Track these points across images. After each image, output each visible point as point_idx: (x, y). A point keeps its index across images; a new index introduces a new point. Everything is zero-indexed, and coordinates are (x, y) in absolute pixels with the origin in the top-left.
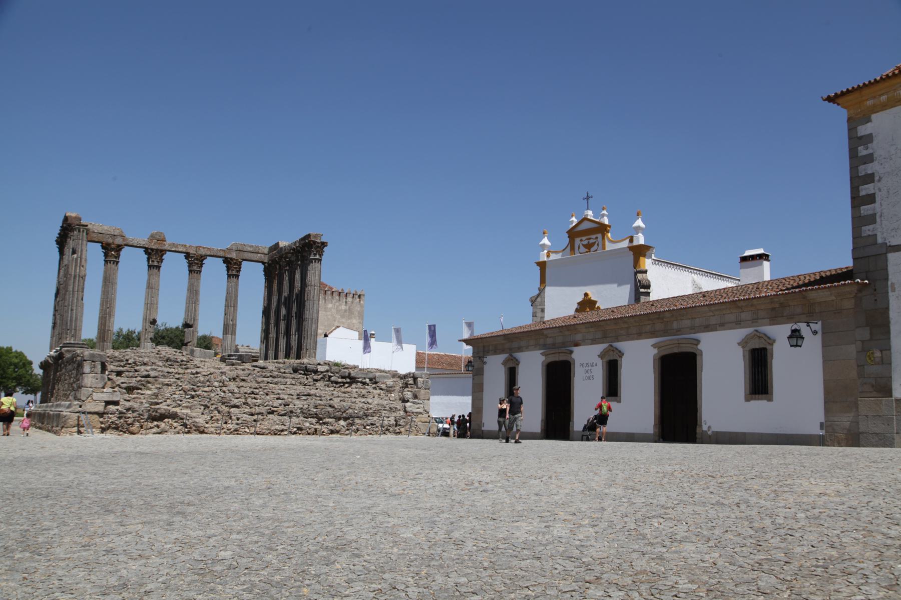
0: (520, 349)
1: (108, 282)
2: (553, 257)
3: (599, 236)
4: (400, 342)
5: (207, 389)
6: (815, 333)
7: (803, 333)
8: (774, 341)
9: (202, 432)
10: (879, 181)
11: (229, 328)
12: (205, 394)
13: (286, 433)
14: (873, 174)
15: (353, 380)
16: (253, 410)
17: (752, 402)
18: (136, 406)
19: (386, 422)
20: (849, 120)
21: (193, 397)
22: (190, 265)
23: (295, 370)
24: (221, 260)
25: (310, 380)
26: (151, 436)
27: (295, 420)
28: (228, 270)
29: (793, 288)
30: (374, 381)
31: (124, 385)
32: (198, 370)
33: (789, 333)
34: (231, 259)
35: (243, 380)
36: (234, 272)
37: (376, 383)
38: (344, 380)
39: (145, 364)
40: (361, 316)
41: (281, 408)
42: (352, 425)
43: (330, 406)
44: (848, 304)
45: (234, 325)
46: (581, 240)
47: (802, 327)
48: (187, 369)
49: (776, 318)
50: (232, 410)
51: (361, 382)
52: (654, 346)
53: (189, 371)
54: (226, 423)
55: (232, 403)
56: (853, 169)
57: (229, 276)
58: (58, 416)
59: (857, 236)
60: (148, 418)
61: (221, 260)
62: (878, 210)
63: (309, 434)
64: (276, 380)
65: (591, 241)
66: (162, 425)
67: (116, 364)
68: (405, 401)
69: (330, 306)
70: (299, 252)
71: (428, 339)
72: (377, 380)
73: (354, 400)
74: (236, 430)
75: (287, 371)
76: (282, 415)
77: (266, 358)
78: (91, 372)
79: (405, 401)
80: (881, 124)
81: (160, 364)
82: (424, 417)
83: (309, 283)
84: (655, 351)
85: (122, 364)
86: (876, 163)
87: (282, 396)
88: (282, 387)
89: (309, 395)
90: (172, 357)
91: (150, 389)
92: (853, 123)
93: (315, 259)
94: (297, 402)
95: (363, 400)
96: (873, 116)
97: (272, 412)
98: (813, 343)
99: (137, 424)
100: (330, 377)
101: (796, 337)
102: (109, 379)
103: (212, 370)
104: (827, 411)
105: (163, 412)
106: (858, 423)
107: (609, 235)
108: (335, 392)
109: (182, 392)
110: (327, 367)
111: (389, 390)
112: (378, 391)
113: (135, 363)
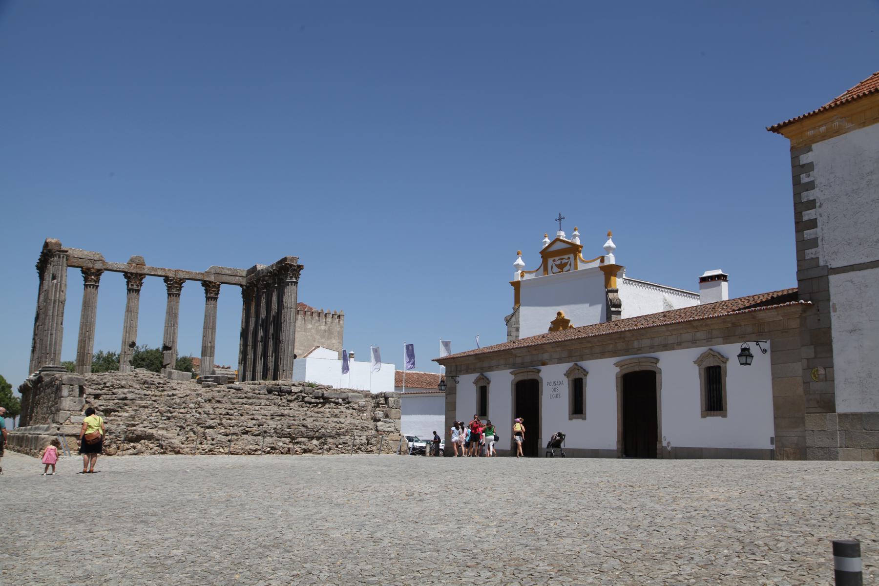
4: (378, 360)
5: (182, 410)
6: (764, 351)
7: (752, 352)
8: (727, 359)
9: (178, 453)
10: (820, 207)
11: (208, 350)
12: (181, 415)
14: (815, 200)
15: (326, 400)
16: (228, 431)
17: (708, 418)
18: (113, 428)
19: (358, 441)
20: (792, 149)
21: (169, 418)
22: (169, 288)
23: (270, 392)
24: (199, 283)
25: (284, 400)
26: (127, 457)
27: (268, 440)
28: (206, 293)
29: (745, 308)
30: (347, 401)
31: (102, 408)
32: (175, 392)
33: (739, 351)
34: (210, 282)
35: (219, 402)
36: (212, 295)
37: (349, 403)
38: (318, 401)
39: (122, 387)
40: (340, 335)
41: (256, 428)
43: (303, 426)
44: (794, 324)
45: (213, 347)
47: (752, 346)
48: (163, 391)
49: (728, 338)
50: (207, 431)
51: (334, 402)
53: (166, 393)
54: (201, 443)
55: (207, 424)
56: (797, 195)
57: (208, 299)
58: (37, 439)
59: (801, 259)
60: (125, 440)
61: (199, 283)
62: (820, 234)
63: (282, 453)
64: (251, 401)
66: (139, 446)
67: (94, 387)
68: (376, 420)
69: (310, 326)
70: (275, 274)
71: (406, 359)
72: (350, 400)
73: (326, 420)
74: (211, 450)
75: (261, 392)
76: (256, 435)
77: (244, 380)
78: (70, 395)
79: (376, 420)
80: (820, 153)
81: (138, 386)
82: (395, 436)
83: (285, 305)
85: (100, 387)
86: (817, 190)
87: (256, 417)
88: (257, 408)
89: (283, 415)
90: (149, 380)
91: (127, 411)
92: (796, 152)
93: (292, 282)
94: (271, 422)
95: (336, 420)
96: (814, 146)
97: (246, 433)
98: (762, 361)
99: (114, 446)
100: (304, 397)
101: (745, 354)
102: (87, 402)
103: (188, 392)
104: (777, 426)
105: (140, 433)
106: (804, 437)
108: (308, 413)
109: (158, 414)
110: (301, 388)
111: (361, 410)
112: (351, 411)
113: (112, 386)
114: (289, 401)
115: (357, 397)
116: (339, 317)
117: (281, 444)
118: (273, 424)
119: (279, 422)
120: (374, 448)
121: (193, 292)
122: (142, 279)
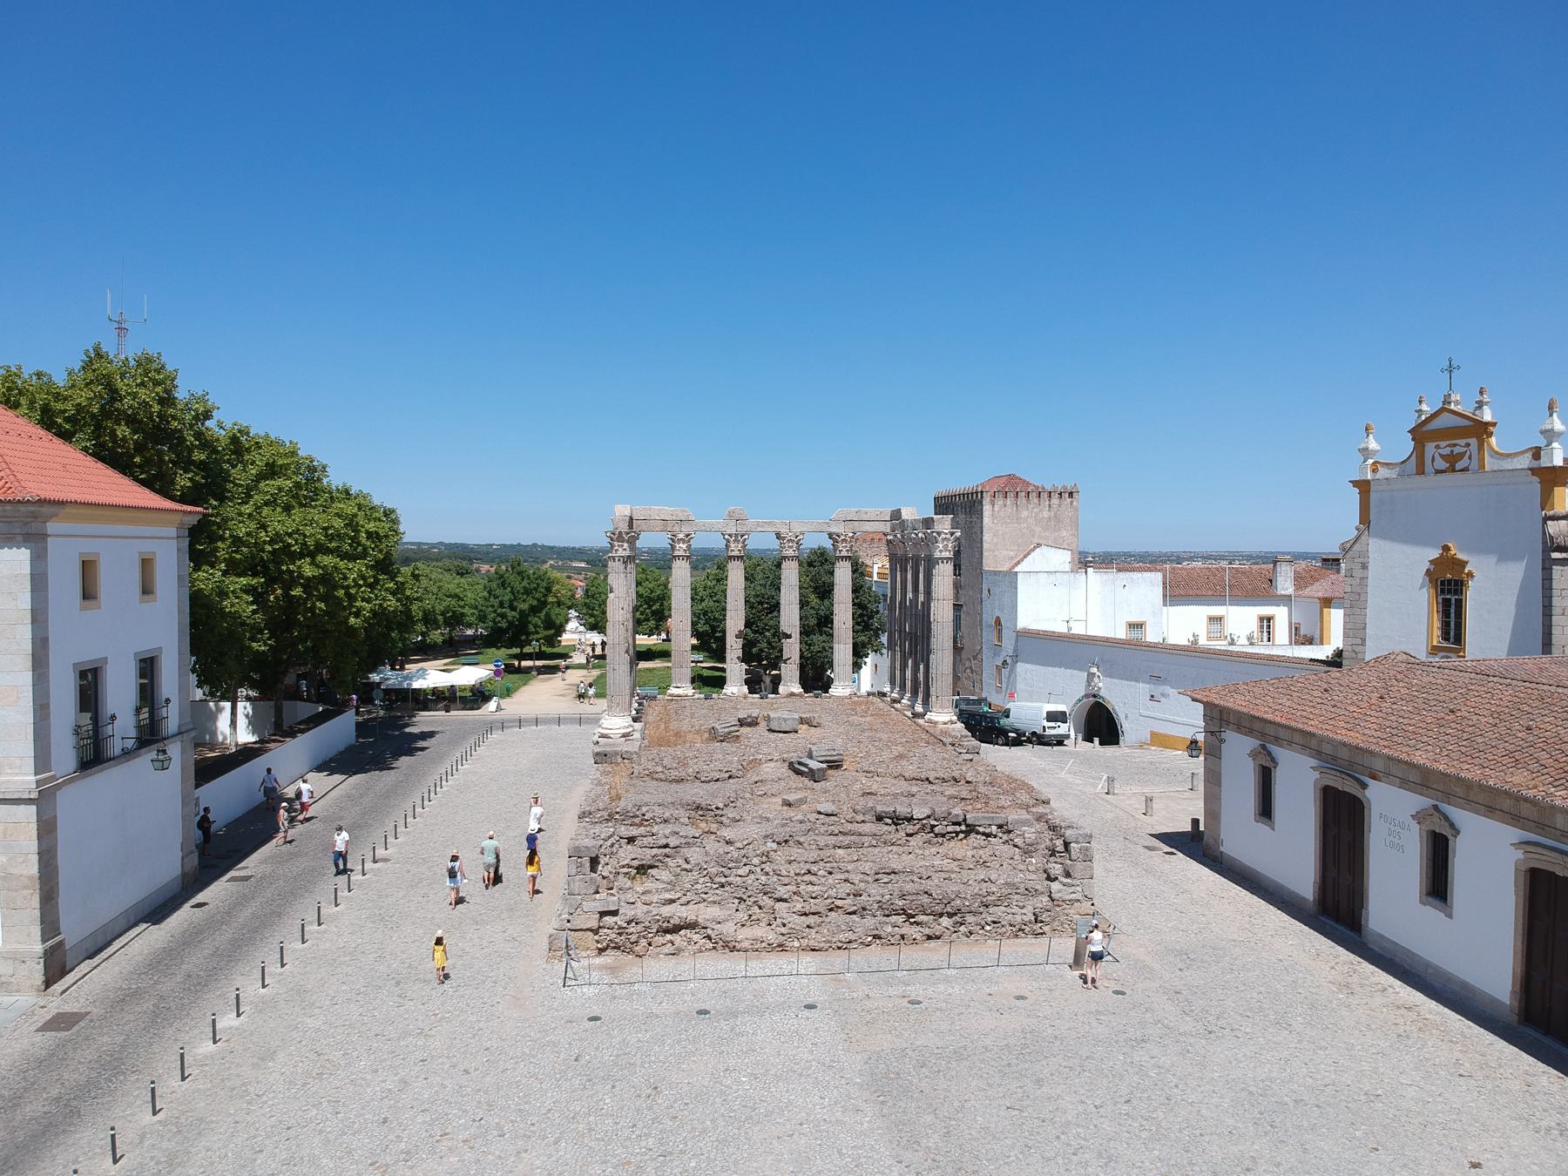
2: (1383, 473)
3: (1473, 441)
5: (740, 872)
19: (1018, 918)
27: (869, 922)
31: (636, 863)
38: (958, 828)
40: (1075, 524)
46: (1437, 447)
50: (778, 905)
52: (1518, 845)
65: (1457, 450)
69: (1025, 514)
84: (1520, 854)
85: (637, 821)
87: (851, 877)
99: (643, 942)
100: (933, 826)
107: (1493, 440)
116: (1071, 494)
117: (889, 929)
118: (875, 891)
120: (1046, 929)
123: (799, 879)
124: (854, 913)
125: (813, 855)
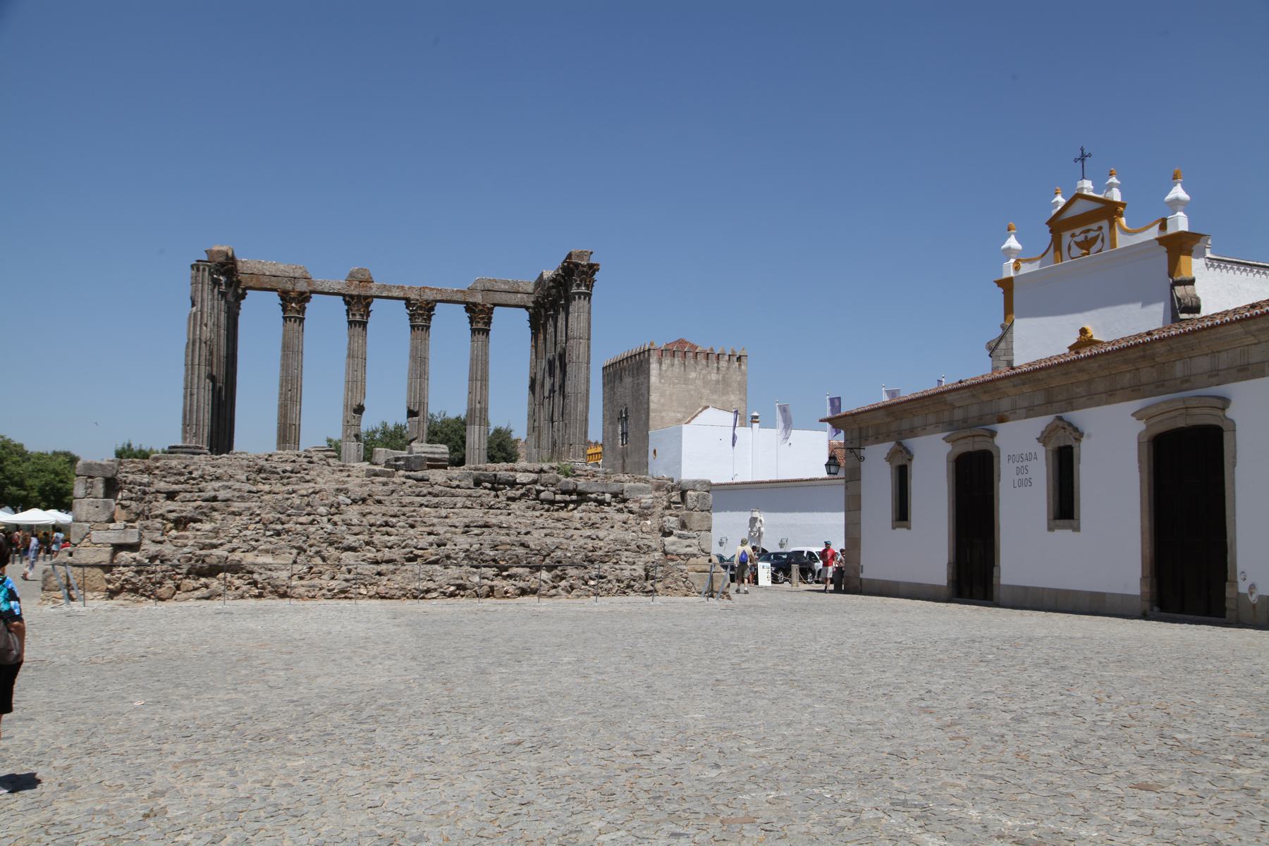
0: (913, 432)
1: (291, 352)
13: (434, 595)
16: (379, 555)
25: (502, 498)
27: (453, 571)
35: (379, 502)
38: (567, 498)
42: (562, 579)
43: (523, 545)
51: (596, 500)
55: (346, 543)
64: (436, 500)
72: (627, 495)
73: (570, 532)
74: (343, 591)
75: (462, 484)
89: (486, 526)
95: (588, 532)
97: (413, 559)
100: (539, 492)
110: (533, 476)
112: (625, 516)
114: (509, 499)
115: (641, 490)
117: (476, 579)
118: (463, 542)
119: (476, 539)
121: (451, 323)
122: (368, 305)
123: (373, 529)
124: (436, 562)
125: (395, 509)
